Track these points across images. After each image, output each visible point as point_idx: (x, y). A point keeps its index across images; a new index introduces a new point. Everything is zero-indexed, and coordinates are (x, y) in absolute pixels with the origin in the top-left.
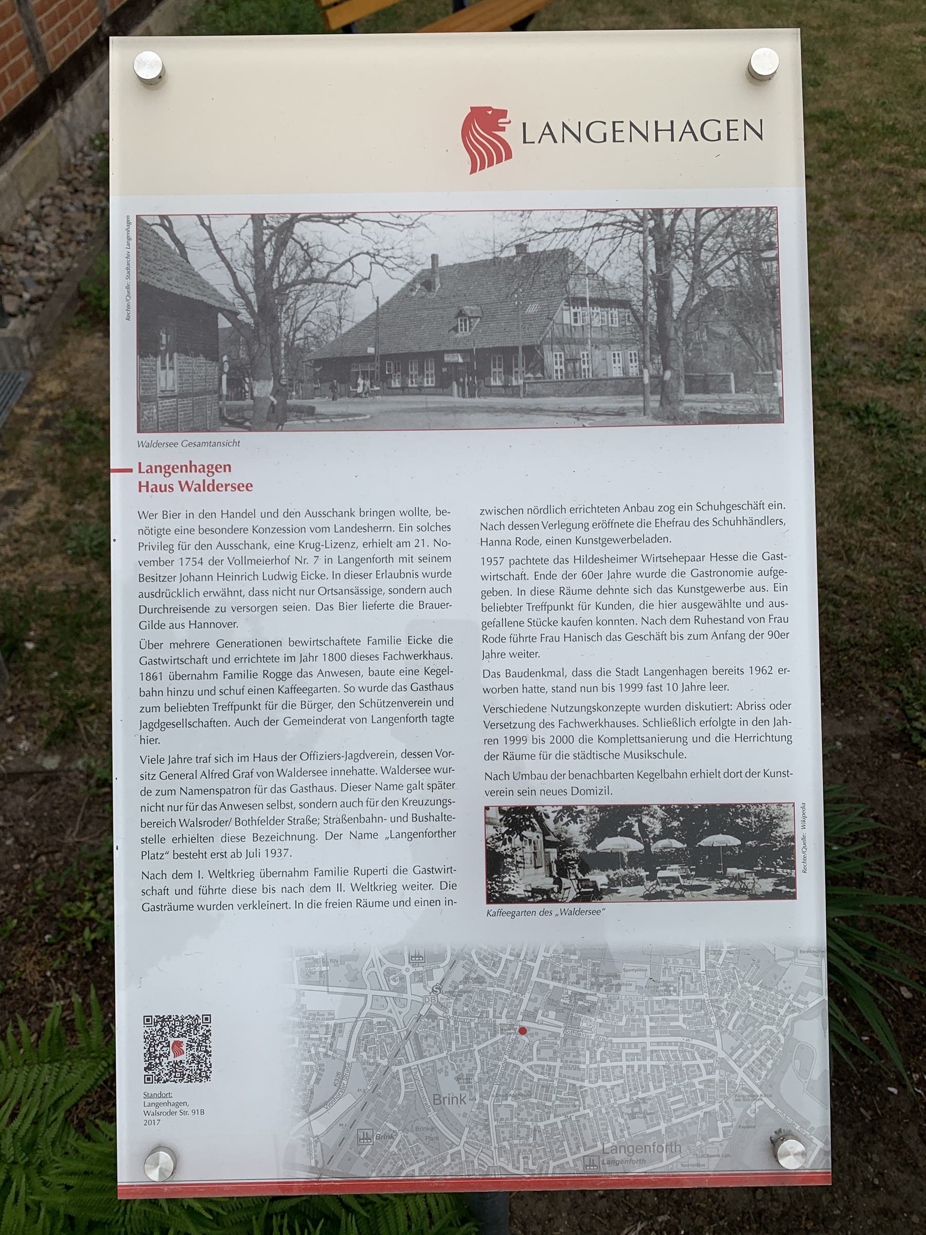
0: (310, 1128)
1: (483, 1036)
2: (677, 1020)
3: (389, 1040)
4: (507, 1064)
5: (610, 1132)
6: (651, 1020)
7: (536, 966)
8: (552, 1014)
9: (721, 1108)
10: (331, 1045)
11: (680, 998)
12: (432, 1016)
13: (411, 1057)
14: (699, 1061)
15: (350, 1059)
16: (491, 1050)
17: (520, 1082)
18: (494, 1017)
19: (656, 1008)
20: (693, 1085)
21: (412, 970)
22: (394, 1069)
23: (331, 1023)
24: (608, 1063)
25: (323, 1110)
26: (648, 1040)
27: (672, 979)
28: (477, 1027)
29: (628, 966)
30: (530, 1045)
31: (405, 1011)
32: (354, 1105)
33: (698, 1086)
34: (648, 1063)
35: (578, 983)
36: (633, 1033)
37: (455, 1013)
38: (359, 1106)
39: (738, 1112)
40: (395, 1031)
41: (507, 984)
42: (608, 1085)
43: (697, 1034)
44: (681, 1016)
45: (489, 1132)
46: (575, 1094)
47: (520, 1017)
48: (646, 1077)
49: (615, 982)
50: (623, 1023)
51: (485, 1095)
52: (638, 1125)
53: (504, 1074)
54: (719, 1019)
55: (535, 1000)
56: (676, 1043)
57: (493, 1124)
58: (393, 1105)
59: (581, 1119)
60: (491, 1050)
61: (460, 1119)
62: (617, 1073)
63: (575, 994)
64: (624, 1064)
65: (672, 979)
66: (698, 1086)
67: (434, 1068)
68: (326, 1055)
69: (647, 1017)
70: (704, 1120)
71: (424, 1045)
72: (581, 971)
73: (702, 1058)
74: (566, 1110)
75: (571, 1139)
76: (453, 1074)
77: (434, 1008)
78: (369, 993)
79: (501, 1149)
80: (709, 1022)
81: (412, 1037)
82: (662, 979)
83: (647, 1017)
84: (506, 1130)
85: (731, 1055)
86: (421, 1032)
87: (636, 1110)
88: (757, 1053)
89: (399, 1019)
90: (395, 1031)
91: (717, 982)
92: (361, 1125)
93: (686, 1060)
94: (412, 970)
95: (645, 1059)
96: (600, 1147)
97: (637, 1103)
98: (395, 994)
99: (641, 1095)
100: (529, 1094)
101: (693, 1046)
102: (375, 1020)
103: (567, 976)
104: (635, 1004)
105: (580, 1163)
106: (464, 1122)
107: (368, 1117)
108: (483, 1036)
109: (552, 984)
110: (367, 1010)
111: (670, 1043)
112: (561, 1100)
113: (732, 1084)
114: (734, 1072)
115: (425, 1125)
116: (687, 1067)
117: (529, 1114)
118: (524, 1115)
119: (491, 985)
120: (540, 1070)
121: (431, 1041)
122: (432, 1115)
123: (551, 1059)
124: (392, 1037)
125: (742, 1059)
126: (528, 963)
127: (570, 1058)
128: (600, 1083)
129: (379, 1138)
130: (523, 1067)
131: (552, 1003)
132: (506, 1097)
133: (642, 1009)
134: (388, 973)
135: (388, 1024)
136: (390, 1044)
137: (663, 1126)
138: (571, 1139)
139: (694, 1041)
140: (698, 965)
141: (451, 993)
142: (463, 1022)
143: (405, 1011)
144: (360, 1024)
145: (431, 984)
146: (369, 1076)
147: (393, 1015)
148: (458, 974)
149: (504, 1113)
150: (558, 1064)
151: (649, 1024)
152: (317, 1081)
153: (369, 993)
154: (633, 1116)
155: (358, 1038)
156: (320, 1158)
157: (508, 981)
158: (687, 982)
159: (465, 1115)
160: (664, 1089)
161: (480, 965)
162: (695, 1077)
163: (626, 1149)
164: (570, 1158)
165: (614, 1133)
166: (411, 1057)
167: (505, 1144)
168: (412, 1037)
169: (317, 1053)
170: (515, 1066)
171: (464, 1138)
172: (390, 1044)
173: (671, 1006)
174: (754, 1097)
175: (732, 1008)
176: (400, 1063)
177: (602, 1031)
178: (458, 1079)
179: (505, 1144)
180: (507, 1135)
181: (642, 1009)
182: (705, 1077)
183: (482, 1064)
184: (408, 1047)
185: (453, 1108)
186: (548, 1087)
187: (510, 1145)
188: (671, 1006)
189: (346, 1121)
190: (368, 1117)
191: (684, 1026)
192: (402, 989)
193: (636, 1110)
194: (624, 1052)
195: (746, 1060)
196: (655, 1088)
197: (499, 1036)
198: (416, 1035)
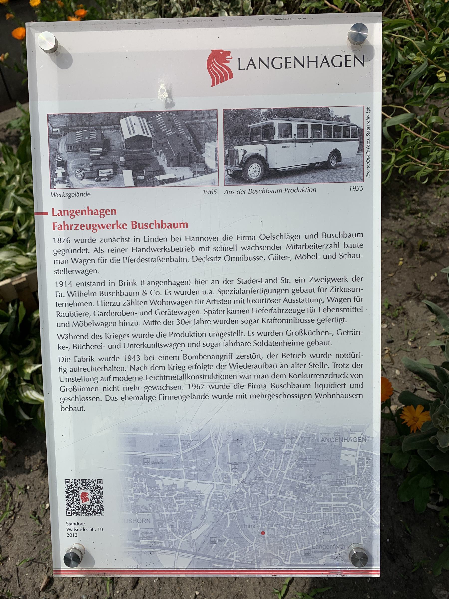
0: (191, 537)
3: (223, 502)
6: (334, 495)
7: (285, 473)
8: (292, 492)
10: (199, 504)
11: (346, 486)
12: (241, 493)
14: (354, 512)
15: (207, 510)
17: (278, 519)
18: (268, 493)
19: (336, 490)
20: (351, 522)
21: (233, 474)
24: (315, 513)
25: (196, 529)
26: (332, 503)
27: (343, 479)
29: (324, 473)
30: (282, 505)
31: (230, 490)
34: (332, 512)
35: (303, 480)
36: (326, 501)
37: (251, 491)
38: (211, 528)
41: (273, 480)
42: (315, 521)
45: (265, 539)
47: (278, 494)
48: (331, 518)
49: (318, 480)
50: (322, 496)
52: (327, 538)
53: (271, 517)
55: (285, 487)
56: (344, 505)
58: (225, 528)
61: (253, 534)
62: (319, 516)
63: (301, 484)
64: (322, 513)
65: (343, 479)
66: (353, 522)
67: (242, 513)
68: (197, 507)
70: (355, 535)
71: (238, 504)
72: (304, 475)
73: (355, 511)
74: (297, 531)
75: (299, 543)
76: (250, 516)
77: (242, 489)
78: (215, 483)
81: (233, 501)
82: (339, 479)
83: (332, 494)
84: (272, 539)
87: (327, 531)
89: (228, 494)
90: (226, 499)
91: (362, 480)
94: (233, 474)
95: (331, 511)
96: (311, 546)
98: (226, 484)
99: (329, 525)
100: (282, 525)
101: (351, 506)
102: (217, 494)
103: (298, 477)
104: (327, 488)
106: (254, 535)
108: (263, 501)
109: (292, 480)
111: (341, 505)
112: (295, 527)
115: (239, 536)
117: (282, 532)
118: (279, 533)
120: (286, 515)
121: (241, 503)
122: (241, 532)
123: (291, 511)
124: (224, 501)
126: (282, 472)
127: (299, 510)
128: (312, 520)
129: (220, 541)
130: (279, 514)
131: (292, 488)
133: (330, 491)
134: (223, 475)
135: (223, 496)
137: (338, 538)
138: (299, 543)
139: (352, 504)
140: (354, 473)
141: (249, 483)
142: (254, 495)
143: (230, 490)
144: (211, 496)
145: (241, 480)
146: (215, 516)
148: (252, 476)
149: (271, 532)
150: (294, 512)
151: (332, 497)
152: (194, 518)
153: (215, 483)
154: (325, 534)
156: (195, 548)
157: (273, 478)
158: (349, 480)
161: (262, 472)
162: (352, 518)
164: (299, 550)
165: (317, 540)
167: (272, 544)
170: (276, 513)
171: (255, 542)
173: (342, 490)
176: (228, 511)
177: (312, 499)
179: (272, 544)
181: (330, 491)
182: (356, 519)
183: (262, 512)
184: (231, 505)
185: (250, 530)
186: (290, 522)
187: (274, 545)
188: (342, 490)
189: (206, 534)
191: (348, 498)
192: (229, 482)
193: (327, 531)
194: (322, 508)
196: (335, 523)
197: (269, 501)
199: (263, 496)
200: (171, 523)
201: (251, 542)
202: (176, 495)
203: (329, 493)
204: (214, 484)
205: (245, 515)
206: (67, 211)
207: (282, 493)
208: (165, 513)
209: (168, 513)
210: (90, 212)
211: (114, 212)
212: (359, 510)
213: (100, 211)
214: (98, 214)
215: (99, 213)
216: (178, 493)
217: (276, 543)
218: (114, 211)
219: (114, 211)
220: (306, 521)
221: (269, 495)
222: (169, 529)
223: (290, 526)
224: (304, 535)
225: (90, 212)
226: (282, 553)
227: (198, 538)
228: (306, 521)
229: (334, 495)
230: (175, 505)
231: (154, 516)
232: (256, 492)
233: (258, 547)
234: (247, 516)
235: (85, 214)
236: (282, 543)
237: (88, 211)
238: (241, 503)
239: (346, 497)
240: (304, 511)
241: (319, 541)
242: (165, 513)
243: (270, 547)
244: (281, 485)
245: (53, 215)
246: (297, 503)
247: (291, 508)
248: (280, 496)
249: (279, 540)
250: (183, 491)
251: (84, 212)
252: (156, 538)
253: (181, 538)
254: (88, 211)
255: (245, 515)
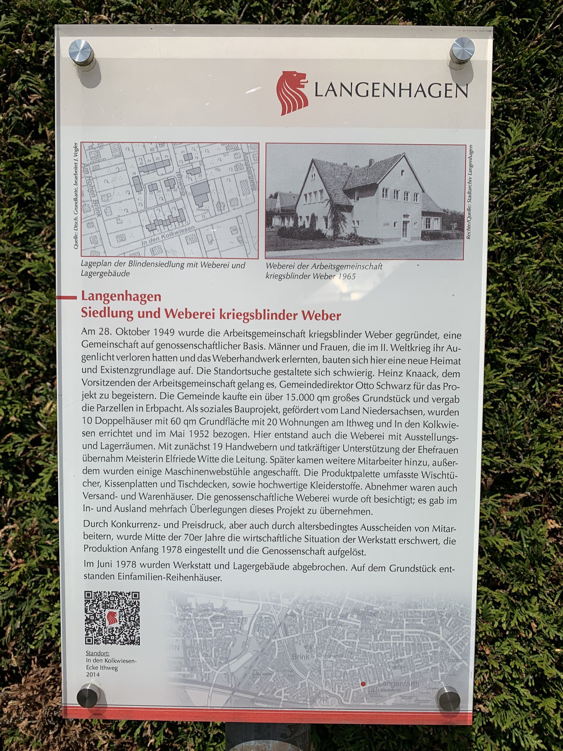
1: (319, 626)
2: (420, 621)
3: (271, 627)
4: (331, 640)
5: (383, 676)
6: (407, 620)
8: (355, 616)
9: (441, 665)
11: (422, 610)
12: (293, 615)
13: (281, 635)
14: (431, 643)
15: (250, 635)
16: (323, 633)
19: (409, 614)
22: (273, 641)
23: (241, 617)
24: (383, 641)
26: (405, 630)
28: (316, 621)
30: (343, 631)
32: (252, 658)
33: (429, 654)
34: (404, 642)
35: (369, 601)
37: (305, 614)
38: (254, 659)
39: (449, 668)
40: (274, 622)
42: (383, 652)
43: (430, 628)
44: (422, 619)
45: (320, 674)
46: (366, 656)
47: (339, 617)
48: (403, 649)
50: (392, 622)
51: (319, 655)
54: (442, 620)
56: (419, 633)
57: (323, 669)
58: (272, 658)
59: (369, 670)
60: (323, 633)
63: (367, 606)
64: (392, 642)
67: (293, 641)
68: (238, 633)
69: (405, 619)
71: (289, 630)
74: (360, 664)
76: (303, 645)
77: (294, 611)
79: (327, 682)
80: (437, 623)
81: (282, 625)
83: (405, 619)
84: (330, 673)
85: (447, 639)
86: (287, 622)
88: (461, 639)
90: (274, 622)
92: (255, 668)
93: (424, 641)
95: (402, 640)
96: (377, 683)
97: (397, 661)
99: (399, 658)
101: (428, 634)
102: (264, 616)
104: (398, 612)
105: (367, 692)
106: (307, 667)
107: (259, 663)
108: (319, 626)
110: (259, 611)
111: (416, 632)
113: (447, 654)
114: (448, 647)
116: (424, 644)
117: (342, 665)
118: (339, 666)
119: (324, 601)
121: (292, 628)
122: (292, 664)
123: (354, 638)
124: (272, 625)
125: (453, 641)
127: (364, 638)
128: (379, 651)
129: (264, 674)
130: (339, 642)
132: (330, 656)
136: (271, 629)
137: (410, 673)
139: (428, 632)
143: (279, 612)
144: (255, 618)
147: (273, 614)
149: (329, 664)
150: (357, 641)
151: (405, 623)
152: (233, 645)
154: (395, 668)
155: (255, 626)
159: (308, 665)
160: (411, 655)
163: (391, 684)
165: (385, 676)
166: (281, 635)
167: (329, 679)
168: (282, 625)
169: (233, 632)
171: (308, 676)
172: (271, 629)
173: (418, 614)
174: (458, 660)
175: (449, 616)
176: (276, 638)
177: (381, 625)
178: (305, 647)
179: (329, 679)
180: (330, 675)
182: (433, 650)
184: (281, 631)
185: (303, 661)
186: (351, 653)
189: (247, 665)
190: (259, 663)
195: (455, 642)
197: (327, 626)
198: (285, 624)
199: (319, 620)
200: (205, 651)
201: (302, 676)
202: (212, 616)
203: (400, 617)
204: (259, 604)
205: (297, 643)
206: (100, 295)
207: (344, 616)
208: (198, 639)
209: (202, 639)
210: (129, 297)
211: (158, 297)
212: (437, 639)
213: (141, 296)
214: (138, 300)
215: (140, 299)
216: (214, 613)
217: (334, 679)
218: (158, 297)
219: (158, 297)
220: (372, 651)
221: (327, 619)
222: (202, 658)
223: (352, 658)
224: (369, 670)
225: (129, 297)
226: (341, 691)
227: (238, 670)
228: (372, 651)
229: (407, 620)
230: (210, 630)
231: (184, 641)
232: (311, 615)
233: (313, 683)
234: (300, 644)
235: (123, 299)
236: (342, 678)
237: (126, 296)
238: (292, 628)
239: (422, 622)
240: (369, 639)
241: (387, 676)
242: (198, 639)
243: (327, 683)
244: (343, 606)
245: (83, 299)
246: (361, 629)
247: (354, 635)
248: (341, 620)
249: (338, 674)
250: (221, 612)
251: (121, 296)
252: (186, 669)
253: (217, 670)
254: (126, 296)
255: (297, 643)
